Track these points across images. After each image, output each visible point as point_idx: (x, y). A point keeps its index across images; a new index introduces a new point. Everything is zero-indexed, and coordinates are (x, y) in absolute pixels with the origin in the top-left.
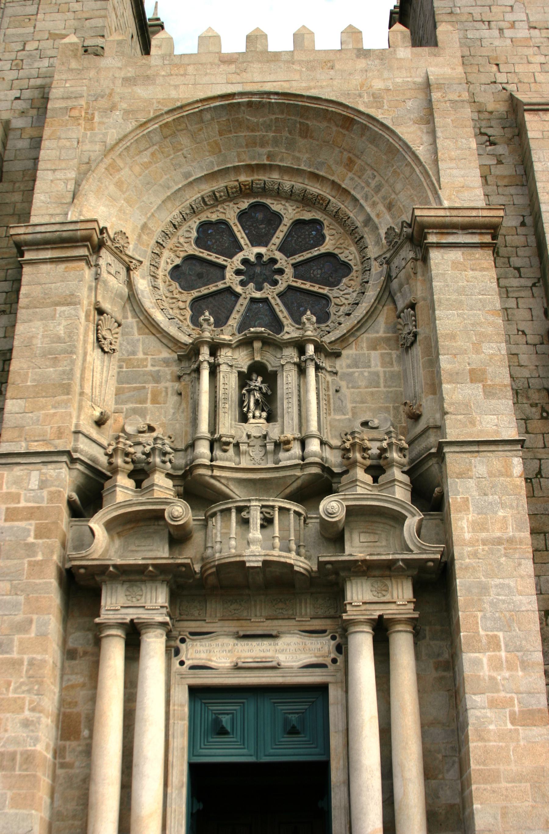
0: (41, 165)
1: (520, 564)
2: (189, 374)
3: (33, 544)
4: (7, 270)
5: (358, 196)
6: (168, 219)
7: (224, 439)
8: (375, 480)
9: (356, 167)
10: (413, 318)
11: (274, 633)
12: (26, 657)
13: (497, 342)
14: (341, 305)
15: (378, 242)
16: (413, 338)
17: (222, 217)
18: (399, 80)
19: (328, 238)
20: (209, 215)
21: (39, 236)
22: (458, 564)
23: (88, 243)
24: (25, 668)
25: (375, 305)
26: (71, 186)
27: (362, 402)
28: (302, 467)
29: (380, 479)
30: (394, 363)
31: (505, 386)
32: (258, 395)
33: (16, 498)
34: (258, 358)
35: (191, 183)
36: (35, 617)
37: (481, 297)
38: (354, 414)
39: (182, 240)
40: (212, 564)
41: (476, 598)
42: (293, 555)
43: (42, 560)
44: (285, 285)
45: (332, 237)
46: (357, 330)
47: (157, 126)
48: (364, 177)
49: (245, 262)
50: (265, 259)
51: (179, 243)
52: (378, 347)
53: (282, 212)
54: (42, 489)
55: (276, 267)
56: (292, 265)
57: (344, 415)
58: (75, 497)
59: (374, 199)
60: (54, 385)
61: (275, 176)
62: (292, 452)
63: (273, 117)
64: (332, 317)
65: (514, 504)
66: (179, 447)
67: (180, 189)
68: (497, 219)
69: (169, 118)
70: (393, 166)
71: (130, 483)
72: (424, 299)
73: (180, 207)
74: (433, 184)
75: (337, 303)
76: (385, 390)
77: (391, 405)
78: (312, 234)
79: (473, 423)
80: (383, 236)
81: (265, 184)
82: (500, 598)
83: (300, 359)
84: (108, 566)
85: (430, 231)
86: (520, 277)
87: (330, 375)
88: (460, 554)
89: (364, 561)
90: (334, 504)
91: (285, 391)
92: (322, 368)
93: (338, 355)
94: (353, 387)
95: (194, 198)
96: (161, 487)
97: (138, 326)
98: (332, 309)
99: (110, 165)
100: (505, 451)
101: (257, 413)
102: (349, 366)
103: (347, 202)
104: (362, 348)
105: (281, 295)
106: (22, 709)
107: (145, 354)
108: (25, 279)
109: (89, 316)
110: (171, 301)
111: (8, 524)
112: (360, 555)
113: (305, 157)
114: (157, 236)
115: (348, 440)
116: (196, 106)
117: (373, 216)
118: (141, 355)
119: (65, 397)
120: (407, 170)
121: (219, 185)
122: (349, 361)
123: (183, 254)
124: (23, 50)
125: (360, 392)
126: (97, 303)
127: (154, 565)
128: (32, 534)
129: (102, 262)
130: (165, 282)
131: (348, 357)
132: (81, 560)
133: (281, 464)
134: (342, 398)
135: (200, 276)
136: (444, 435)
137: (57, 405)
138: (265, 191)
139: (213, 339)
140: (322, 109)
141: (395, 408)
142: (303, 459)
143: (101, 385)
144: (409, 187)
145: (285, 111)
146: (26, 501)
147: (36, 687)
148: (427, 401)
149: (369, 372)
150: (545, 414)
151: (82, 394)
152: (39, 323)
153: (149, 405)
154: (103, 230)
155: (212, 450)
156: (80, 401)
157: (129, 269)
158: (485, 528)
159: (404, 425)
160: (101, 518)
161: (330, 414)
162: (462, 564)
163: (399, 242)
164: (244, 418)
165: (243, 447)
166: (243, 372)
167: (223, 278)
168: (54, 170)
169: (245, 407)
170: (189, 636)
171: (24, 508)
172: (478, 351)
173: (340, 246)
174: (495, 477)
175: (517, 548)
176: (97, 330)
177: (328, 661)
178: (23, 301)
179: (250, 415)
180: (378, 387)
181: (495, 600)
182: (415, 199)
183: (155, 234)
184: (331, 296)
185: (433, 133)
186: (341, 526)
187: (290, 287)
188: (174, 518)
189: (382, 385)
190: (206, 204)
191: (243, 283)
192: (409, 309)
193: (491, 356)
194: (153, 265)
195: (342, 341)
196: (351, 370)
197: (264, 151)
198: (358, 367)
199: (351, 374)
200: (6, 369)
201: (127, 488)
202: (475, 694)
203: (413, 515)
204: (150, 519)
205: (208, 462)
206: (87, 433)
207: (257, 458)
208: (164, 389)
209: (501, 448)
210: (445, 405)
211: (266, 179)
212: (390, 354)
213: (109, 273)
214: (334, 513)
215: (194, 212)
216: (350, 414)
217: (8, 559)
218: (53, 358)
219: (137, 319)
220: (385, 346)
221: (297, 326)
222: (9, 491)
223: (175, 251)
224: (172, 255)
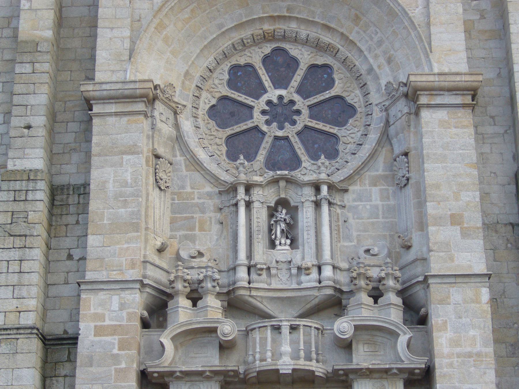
0: (101, 23)
1: (485, 373)
2: (229, 207)
3: (118, 355)
4: (75, 111)
5: (363, 48)
6: (205, 65)
7: (259, 266)
8: (376, 302)
9: (361, 23)
10: (407, 165)
13: (472, 191)
14: (348, 144)
15: (378, 90)
16: (406, 181)
17: (249, 61)
19: (337, 83)
20: (238, 59)
21: (105, 93)
22: (438, 372)
23: (145, 99)
25: (376, 148)
26: (127, 44)
27: (365, 231)
28: (320, 288)
29: (380, 300)
30: (391, 198)
31: (478, 228)
32: (283, 226)
33: (101, 317)
34: (283, 196)
35: (224, 33)
37: (461, 151)
38: (359, 241)
39: (217, 82)
40: (254, 370)
42: (314, 363)
45: (340, 81)
46: (361, 170)
48: (368, 32)
49: (269, 103)
50: (286, 101)
51: (214, 84)
52: (378, 184)
53: (299, 57)
54: (122, 310)
55: (295, 108)
57: (351, 242)
58: (146, 314)
59: (376, 52)
61: (293, 25)
62: (311, 276)
64: (341, 154)
65: (482, 326)
66: (223, 269)
67: (214, 39)
70: (392, 27)
71: (188, 303)
72: (416, 149)
73: (214, 54)
74: (426, 49)
75: (345, 142)
76: (383, 220)
77: (388, 234)
78: (324, 77)
79: (452, 259)
80: (384, 88)
81: (285, 32)
83: (316, 198)
84: (175, 372)
85: (422, 93)
86: (495, 125)
87: (340, 209)
88: (439, 364)
89: (368, 369)
90: (345, 324)
91: (305, 224)
92: (334, 204)
93: (346, 191)
94: (357, 218)
95: (226, 45)
96: (213, 307)
97: (185, 163)
98: (341, 147)
99: (158, 24)
101: (283, 241)
102: (354, 200)
104: (365, 184)
105: (299, 134)
107: (192, 188)
108: (95, 129)
109: (149, 161)
110: (210, 138)
111: (97, 339)
112: (365, 365)
114: (196, 81)
115: (355, 270)
117: (375, 67)
118: (188, 189)
119: (135, 234)
121: (246, 33)
122: (354, 196)
123: (218, 95)
125: (363, 222)
126: (154, 150)
127: (211, 371)
128: (116, 347)
129: (156, 114)
130: (204, 120)
132: (155, 367)
133: (303, 286)
135: (232, 114)
136: (428, 268)
137: (129, 240)
138: (284, 38)
139: (248, 181)
141: (391, 236)
142: (320, 282)
143: (160, 219)
144: (405, 47)
146: (111, 319)
148: (416, 236)
149: (370, 205)
150: (509, 245)
151: (147, 229)
152: (109, 170)
153: (197, 232)
154: (156, 87)
155: (249, 274)
156: (146, 235)
157: (175, 113)
158: (459, 345)
159: (398, 250)
160: (169, 334)
161: (340, 241)
162: (441, 372)
163: (397, 95)
164: (272, 245)
165: (273, 271)
167: (252, 117)
168: (112, 29)
169: (273, 235)
171: (108, 325)
172: (457, 198)
173: (347, 89)
174: (468, 303)
175: (483, 360)
176: (156, 173)
178: (95, 149)
179: (277, 242)
180: (378, 218)
182: (411, 58)
183: (195, 78)
184: (339, 135)
186: (350, 340)
187: (306, 127)
188: (224, 335)
189: (381, 216)
190: (235, 49)
191: (268, 123)
192: (404, 157)
194: (195, 107)
195: (350, 179)
196: (356, 203)
198: (361, 201)
199: (356, 207)
200: (82, 201)
201: (186, 308)
203: (405, 333)
204: (205, 332)
205: (247, 285)
206: (152, 261)
207: (284, 279)
208: (208, 219)
209: (473, 280)
210: (430, 245)
211: (286, 28)
212: (387, 190)
213: (162, 121)
214: (345, 332)
215: (226, 57)
216: (355, 241)
217: (98, 366)
218: (123, 201)
219: (185, 158)
221: (313, 162)
222: (96, 311)
223: (211, 92)
224: (209, 96)
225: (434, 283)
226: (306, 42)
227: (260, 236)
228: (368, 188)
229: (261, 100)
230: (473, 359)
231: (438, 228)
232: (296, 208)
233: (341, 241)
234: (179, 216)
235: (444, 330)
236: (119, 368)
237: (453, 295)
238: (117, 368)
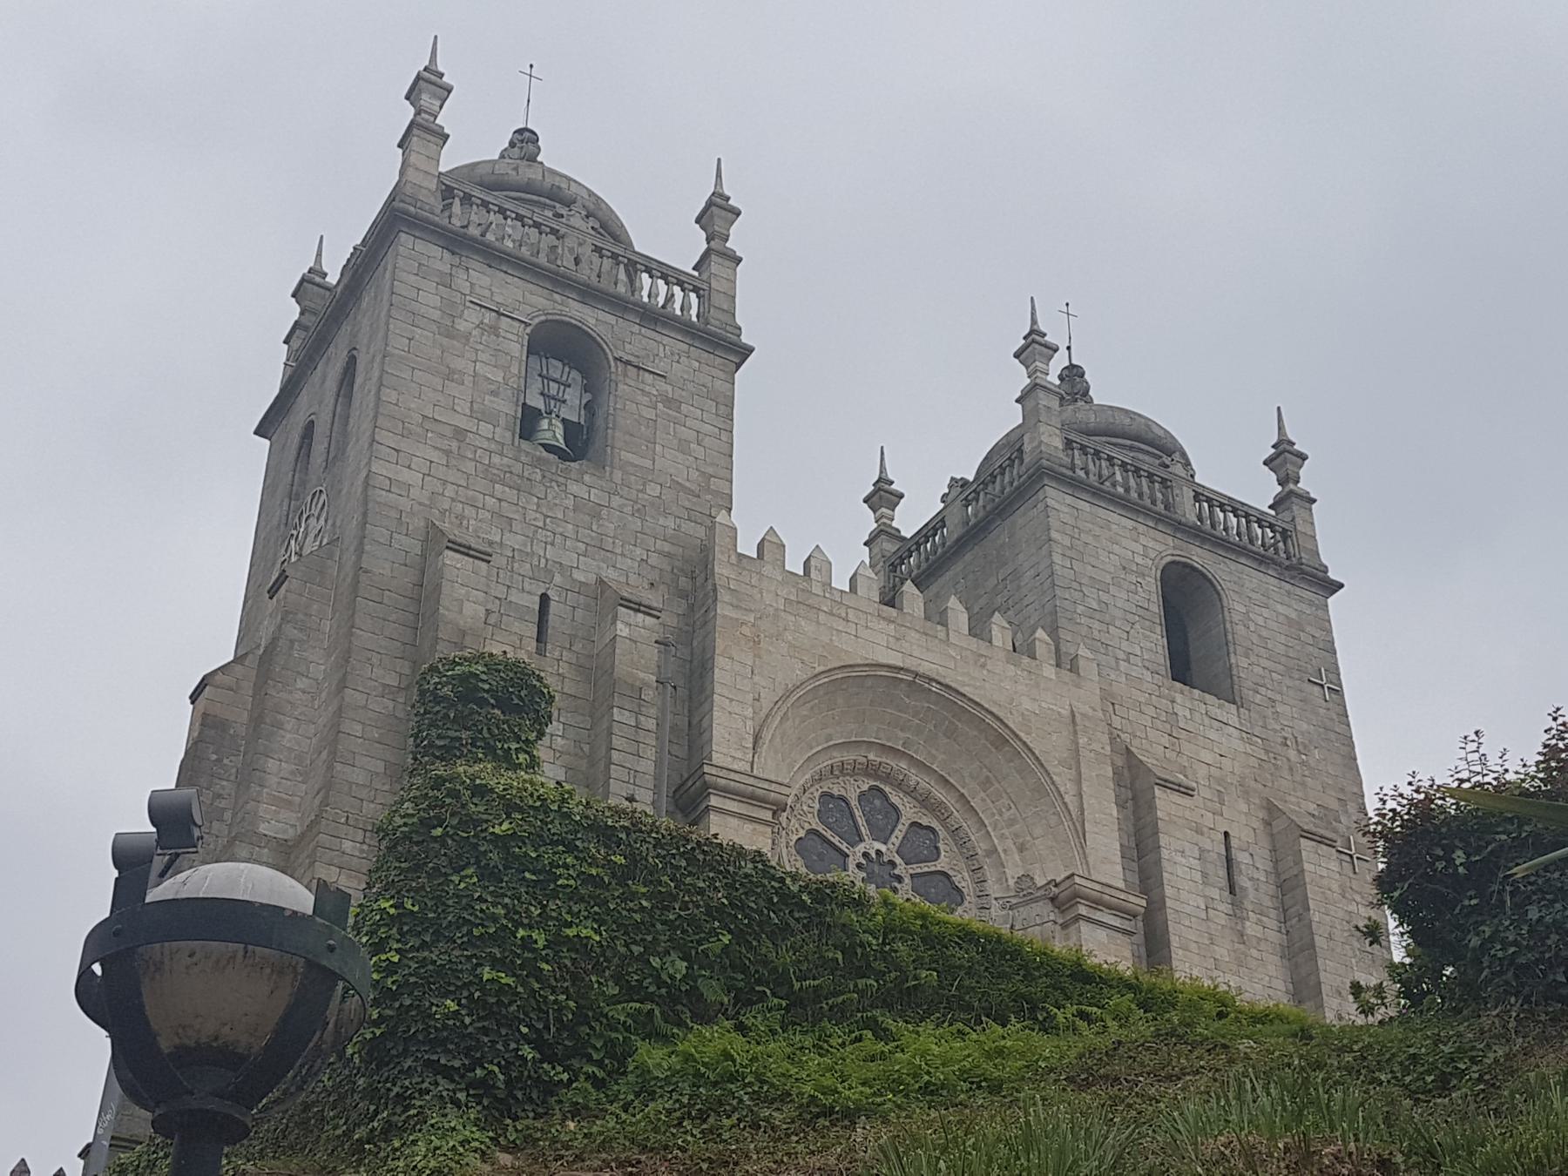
5: (986, 822)
15: (999, 880)
18: (1043, 704)
19: (943, 853)
47: (826, 680)
53: (901, 807)
63: (927, 705)
95: (825, 764)
113: (941, 757)
117: (1000, 849)
120: (1053, 820)
121: (849, 756)
123: (807, 826)
124: (643, 491)
138: (887, 778)
185: (1078, 781)
223: (799, 819)
224: (797, 826)
226: (911, 792)
229: (857, 849)
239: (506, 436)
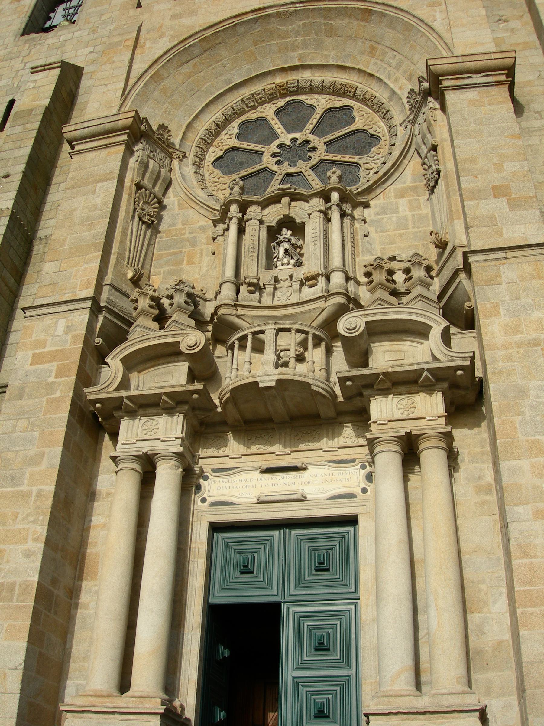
6: (212, 120)
11: (299, 465)
12: (35, 489)
14: (371, 169)
16: (437, 176)
23: (128, 131)
24: (33, 499)
27: (391, 243)
36: (47, 450)
37: (499, 125)
40: (227, 390)
41: (512, 402)
43: (60, 397)
44: (317, 159)
45: (361, 118)
52: (405, 195)
54: (67, 334)
56: (325, 143)
59: (396, 75)
60: (88, 245)
61: (307, 74)
63: (302, 22)
68: (509, 59)
69: (209, 33)
73: (222, 110)
80: (405, 100)
81: (298, 82)
82: (541, 400)
89: (386, 374)
93: (366, 205)
94: (381, 232)
95: (235, 101)
97: (178, 203)
100: (537, 255)
102: (377, 214)
103: (373, 84)
104: (390, 197)
106: (26, 539)
107: (183, 224)
116: (231, 21)
117: (396, 90)
120: (422, 41)
122: (377, 210)
125: (389, 235)
128: (54, 374)
131: (376, 207)
134: (371, 242)
138: (299, 90)
140: (343, 7)
145: (311, 16)
147: (41, 518)
149: (397, 217)
153: (185, 266)
158: (519, 331)
162: (494, 369)
166: (272, 227)
168: (106, 85)
170: (211, 473)
171: (48, 352)
174: (526, 280)
177: (358, 491)
179: (279, 263)
181: (534, 403)
184: (361, 162)
193: (514, 174)
196: (379, 217)
197: (296, 54)
198: (385, 213)
199: (379, 221)
202: (516, 505)
208: (199, 251)
211: (299, 79)
214: (354, 328)
217: (29, 398)
220: (412, 193)
222: (37, 338)
225: (477, 261)
226: (322, 90)
227: (255, 254)
228: (393, 200)
230: (540, 348)
231: (476, 202)
232: (302, 226)
233: (360, 255)
234: (165, 252)
235: (495, 316)
236: (53, 398)
237: (504, 273)
238: (50, 398)
239: (10, 40)
